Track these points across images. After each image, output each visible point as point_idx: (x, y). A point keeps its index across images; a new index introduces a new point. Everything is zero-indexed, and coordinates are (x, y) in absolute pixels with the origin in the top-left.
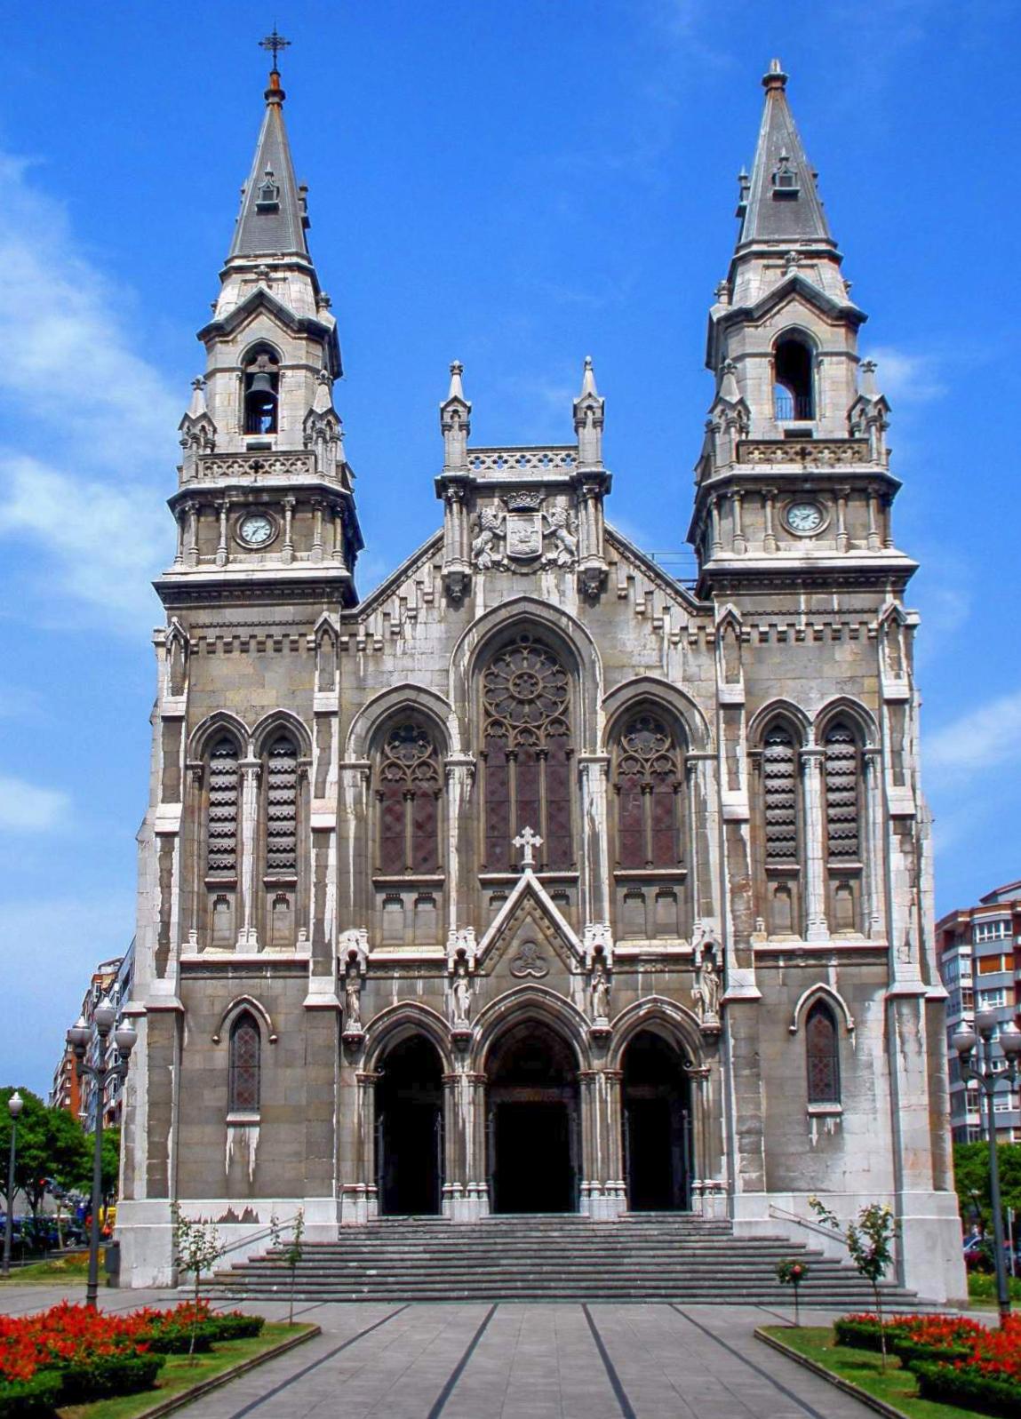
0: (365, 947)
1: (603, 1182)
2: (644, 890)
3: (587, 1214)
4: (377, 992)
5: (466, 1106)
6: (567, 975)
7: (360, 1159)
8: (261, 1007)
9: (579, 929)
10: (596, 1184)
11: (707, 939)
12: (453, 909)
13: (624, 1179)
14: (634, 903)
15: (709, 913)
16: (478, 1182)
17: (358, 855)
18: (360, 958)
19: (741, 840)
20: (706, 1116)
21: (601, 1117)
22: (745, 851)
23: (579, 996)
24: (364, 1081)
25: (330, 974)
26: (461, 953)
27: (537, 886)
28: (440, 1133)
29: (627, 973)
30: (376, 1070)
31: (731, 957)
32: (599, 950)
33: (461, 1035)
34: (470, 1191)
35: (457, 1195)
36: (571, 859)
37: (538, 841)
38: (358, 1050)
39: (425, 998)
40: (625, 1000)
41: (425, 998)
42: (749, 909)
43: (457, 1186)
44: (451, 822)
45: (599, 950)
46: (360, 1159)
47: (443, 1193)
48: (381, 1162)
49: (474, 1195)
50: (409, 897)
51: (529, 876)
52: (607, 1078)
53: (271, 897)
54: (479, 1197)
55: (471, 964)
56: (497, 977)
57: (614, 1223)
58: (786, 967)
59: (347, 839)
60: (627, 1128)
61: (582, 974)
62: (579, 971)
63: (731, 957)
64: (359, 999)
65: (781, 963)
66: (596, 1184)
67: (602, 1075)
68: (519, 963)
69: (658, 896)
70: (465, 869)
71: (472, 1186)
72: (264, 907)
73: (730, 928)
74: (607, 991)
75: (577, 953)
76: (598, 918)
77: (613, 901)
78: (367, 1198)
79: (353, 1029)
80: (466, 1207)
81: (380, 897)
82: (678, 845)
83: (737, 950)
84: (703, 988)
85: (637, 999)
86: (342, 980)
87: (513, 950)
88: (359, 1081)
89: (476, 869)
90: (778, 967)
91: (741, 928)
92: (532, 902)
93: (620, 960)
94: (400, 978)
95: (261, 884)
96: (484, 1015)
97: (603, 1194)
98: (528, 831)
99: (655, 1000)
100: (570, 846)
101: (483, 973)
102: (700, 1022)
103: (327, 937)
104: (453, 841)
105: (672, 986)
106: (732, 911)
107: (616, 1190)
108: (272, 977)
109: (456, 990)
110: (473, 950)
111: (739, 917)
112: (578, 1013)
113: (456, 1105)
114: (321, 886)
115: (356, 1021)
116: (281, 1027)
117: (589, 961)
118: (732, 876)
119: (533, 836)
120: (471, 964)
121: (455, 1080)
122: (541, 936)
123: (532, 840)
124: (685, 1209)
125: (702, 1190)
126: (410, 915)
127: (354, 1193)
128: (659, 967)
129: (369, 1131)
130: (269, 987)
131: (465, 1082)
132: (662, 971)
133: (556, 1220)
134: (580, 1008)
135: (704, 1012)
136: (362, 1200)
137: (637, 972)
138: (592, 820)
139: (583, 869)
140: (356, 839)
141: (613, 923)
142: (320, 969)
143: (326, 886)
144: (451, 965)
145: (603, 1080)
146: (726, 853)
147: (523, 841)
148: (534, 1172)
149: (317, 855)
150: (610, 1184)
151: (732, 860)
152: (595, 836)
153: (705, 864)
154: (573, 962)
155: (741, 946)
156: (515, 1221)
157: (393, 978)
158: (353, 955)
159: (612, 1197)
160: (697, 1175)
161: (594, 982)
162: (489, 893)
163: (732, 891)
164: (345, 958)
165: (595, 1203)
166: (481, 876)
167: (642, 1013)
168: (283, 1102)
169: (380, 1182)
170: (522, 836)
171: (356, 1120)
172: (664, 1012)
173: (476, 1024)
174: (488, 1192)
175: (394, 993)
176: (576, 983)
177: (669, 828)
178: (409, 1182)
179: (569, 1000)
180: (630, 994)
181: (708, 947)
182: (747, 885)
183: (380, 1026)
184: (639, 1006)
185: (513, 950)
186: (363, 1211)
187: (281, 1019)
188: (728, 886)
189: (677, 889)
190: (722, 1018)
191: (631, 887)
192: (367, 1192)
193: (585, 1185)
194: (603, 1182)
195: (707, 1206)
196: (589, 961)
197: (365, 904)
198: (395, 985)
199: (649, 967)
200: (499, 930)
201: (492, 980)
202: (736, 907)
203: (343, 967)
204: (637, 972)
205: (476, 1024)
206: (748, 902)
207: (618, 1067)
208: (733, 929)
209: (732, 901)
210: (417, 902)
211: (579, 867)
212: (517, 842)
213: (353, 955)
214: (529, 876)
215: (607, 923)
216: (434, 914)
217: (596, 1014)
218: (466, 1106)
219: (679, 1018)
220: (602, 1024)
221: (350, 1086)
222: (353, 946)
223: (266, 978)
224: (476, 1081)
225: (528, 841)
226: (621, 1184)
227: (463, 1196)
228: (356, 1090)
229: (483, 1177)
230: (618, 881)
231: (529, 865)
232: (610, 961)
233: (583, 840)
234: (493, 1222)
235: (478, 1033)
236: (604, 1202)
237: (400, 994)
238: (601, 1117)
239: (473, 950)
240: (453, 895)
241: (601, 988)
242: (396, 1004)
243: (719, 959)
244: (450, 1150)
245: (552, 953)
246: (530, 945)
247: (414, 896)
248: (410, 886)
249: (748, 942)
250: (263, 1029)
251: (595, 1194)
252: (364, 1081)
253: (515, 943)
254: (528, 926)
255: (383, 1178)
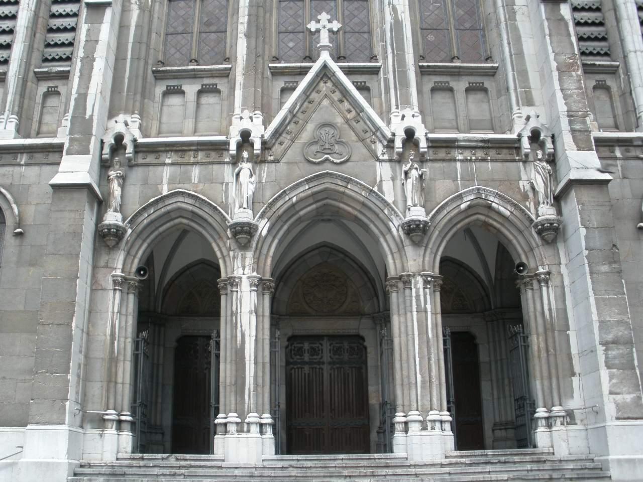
0: (137, 134)
1: (425, 412)
2: (453, 84)
3: (404, 455)
4: (145, 182)
5: (245, 316)
6: (371, 162)
7: (111, 379)
8: (9, 196)
9: (386, 115)
10: (414, 415)
11: (533, 124)
12: (238, 93)
13: (449, 410)
14: (440, 97)
15: (529, 101)
16: (261, 414)
17: (138, 42)
18: (127, 141)
19: (562, 19)
20: (549, 328)
21: (417, 328)
22: (568, 31)
23: (387, 186)
24: (122, 284)
25: (86, 152)
26: (245, 135)
27: (334, 66)
28: (213, 352)
29: (443, 160)
30: (139, 270)
31: (567, 139)
32: (410, 133)
33: (242, 225)
34: (248, 424)
35: (232, 428)
36: (371, 49)
37: (336, 26)
38: (116, 246)
39: (201, 186)
40: (442, 189)
41: (201, 186)
42: (581, 88)
43: (233, 417)
44: (241, 10)
45: (410, 133)
46: (111, 379)
47: (215, 425)
48: (140, 385)
49: (255, 429)
50: (191, 89)
51: (325, 57)
52: (426, 282)
53: (43, 88)
54: (261, 432)
55: (258, 145)
56: (288, 163)
57: (442, 465)
58: (626, 158)
59: (128, 27)
60: (449, 346)
61: (390, 161)
62: (386, 157)
63: (567, 139)
64: (123, 187)
65: (618, 154)
66: (414, 415)
67: (420, 280)
68: (315, 148)
69: (468, 90)
70: (254, 55)
71: (252, 417)
72: (32, 98)
73: (562, 107)
74: (421, 176)
75: (384, 136)
76: (406, 102)
77: (420, 92)
78: (119, 429)
79: (112, 218)
80: (245, 442)
81: (160, 88)
82: (485, 42)
83: (573, 131)
84: (534, 176)
85: (460, 185)
86: (105, 165)
87: (306, 136)
88: (115, 282)
89: (266, 58)
90: (616, 158)
91: (574, 108)
92: (329, 84)
93: (435, 144)
94: (172, 164)
95: (31, 74)
96: (271, 205)
97: (424, 428)
98: (324, 17)
99: (478, 189)
100: (370, 40)
101: (271, 158)
102: (533, 217)
103: (89, 113)
104: (242, 28)
105: (496, 177)
106: (562, 90)
107: (441, 422)
108: (27, 165)
109: (238, 175)
110: (259, 132)
111: (571, 96)
112: (387, 204)
113: (234, 314)
114: (89, 61)
115: (116, 211)
116: (29, 219)
117: (398, 144)
118: (556, 54)
119: (330, 21)
120: (258, 145)
121: (233, 282)
122: (339, 120)
123: (329, 26)
124: (526, 446)
125: (549, 422)
126: (192, 106)
127: (101, 423)
128: (480, 154)
129: (125, 345)
130: (22, 176)
131: (245, 285)
132: (484, 160)
133: (365, 463)
134: (389, 199)
135: (537, 204)
136: (111, 431)
137: (455, 160)
138: (394, 9)
139: (385, 58)
140: (137, 26)
141: (422, 112)
142: (76, 147)
143: (94, 60)
144: (233, 147)
145: (420, 285)
146: (547, 31)
147: (319, 26)
148: (332, 403)
149: (88, 30)
150: (434, 415)
151: (555, 39)
152: (397, 25)
153: (519, 54)
154: (379, 148)
155: (578, 127)
156: (309, 464)
157: (164, 164)
158: (119, 138)
159: (437, 431)
160: (540, 402)
161: (405, 168)
162: (280, 83)
163: (558, 69)
164: (110, 140)
165: (416, 440)
166: (271, 65)
167: (463, 206)
168: (21, 308)
169: (138, 411)
170: (318, 21)
171: (108, 332)
172: (490, 207)
173: (262, 217)
174: (274, 426)
175: (165, 181)
176: (384, 171)
177: (472, 29)
178: (175, 404)
179: (376, 189)
180: (449, 184)
181: (535, 137)
182: (572, 65)
183: (145, 219)
184: (460, 197)
185: (306, 136)
186: (114, 445)
187: (30, 212)
188: (554, 65)
189: (488, 83)
190: (559, 212)
191: (437, 76)
192: (120, 422)
193: (399, 418)
194: (425, 412)
195: (555, 440)
196: (398, 144)
197: (145, 94)
198: (166, 173)
199: (468, 154)
200: (291, 111)
201: (282, 166)
202: (565, 86)
203: (107, 150)
204: (455, 160)
205: (262, 217)
206: (579, 81)
207: (437, 270)
208: (565, 108)
209: (560, 80)
210: (200, 93)
211: (380, 57)
212: (313, 26)
213: (119, 138)
214: (325, 57)
215: (416, 109)
216: (218, 107)
217: (409, 203)
218: (245, 316)
219: (508, 213)
220: (418, 214)
221: (105, 289)
222: (120, 128)
223: (20, 165)
224: (260, 285)
225: (324, 25)
226: (446, 416)
227: (240, 431)
228: (111, 293)
229: (267, 407)
230: (423, 72)
231: (325, 47)
232: (423, 144)
233: (383, 31)
234: (280, 464)
235: (263, 227)
236: (424, 438)
237: (171, 182)
238: (417, 328)
239: (259, 132)
240: (240, 79)
241: (414, 174)
242: (165, 192)
243: (549, 145)
244: (226, 371)
245: (354, 138)
246: (327, 129)
247: (197, 87)
248: (194, 75)
249: (584, 123)
250: (9, 221)
251: (415, 428)
252: (122, 284)
253: (310, 127)
254: (326, 109)
255: (142, 404)
